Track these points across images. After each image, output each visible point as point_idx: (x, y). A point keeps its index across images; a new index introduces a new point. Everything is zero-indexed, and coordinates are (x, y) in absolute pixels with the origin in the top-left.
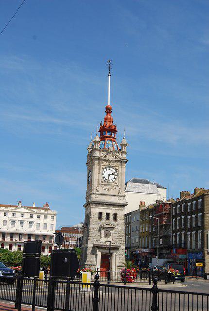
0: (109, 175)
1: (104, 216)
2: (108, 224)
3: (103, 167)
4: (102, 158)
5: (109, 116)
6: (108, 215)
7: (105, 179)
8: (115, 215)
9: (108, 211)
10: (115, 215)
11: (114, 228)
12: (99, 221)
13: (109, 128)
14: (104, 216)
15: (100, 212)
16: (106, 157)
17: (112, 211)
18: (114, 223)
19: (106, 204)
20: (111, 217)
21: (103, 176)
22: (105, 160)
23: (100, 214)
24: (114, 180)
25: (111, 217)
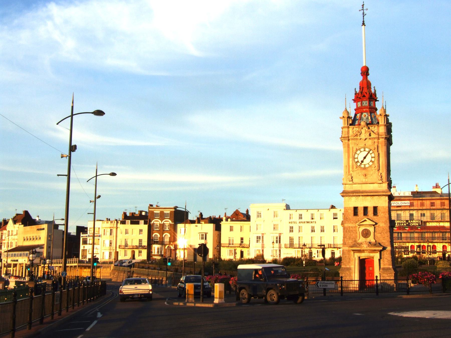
0: (365, 158)
1: (361, 212)
2: (365, 221)
8: (375, 209)
10: (375, 209)
12: (355, 217)
14: (361, 212)
15: (356, 206)
23: (356, 209)
24: (371, 163)
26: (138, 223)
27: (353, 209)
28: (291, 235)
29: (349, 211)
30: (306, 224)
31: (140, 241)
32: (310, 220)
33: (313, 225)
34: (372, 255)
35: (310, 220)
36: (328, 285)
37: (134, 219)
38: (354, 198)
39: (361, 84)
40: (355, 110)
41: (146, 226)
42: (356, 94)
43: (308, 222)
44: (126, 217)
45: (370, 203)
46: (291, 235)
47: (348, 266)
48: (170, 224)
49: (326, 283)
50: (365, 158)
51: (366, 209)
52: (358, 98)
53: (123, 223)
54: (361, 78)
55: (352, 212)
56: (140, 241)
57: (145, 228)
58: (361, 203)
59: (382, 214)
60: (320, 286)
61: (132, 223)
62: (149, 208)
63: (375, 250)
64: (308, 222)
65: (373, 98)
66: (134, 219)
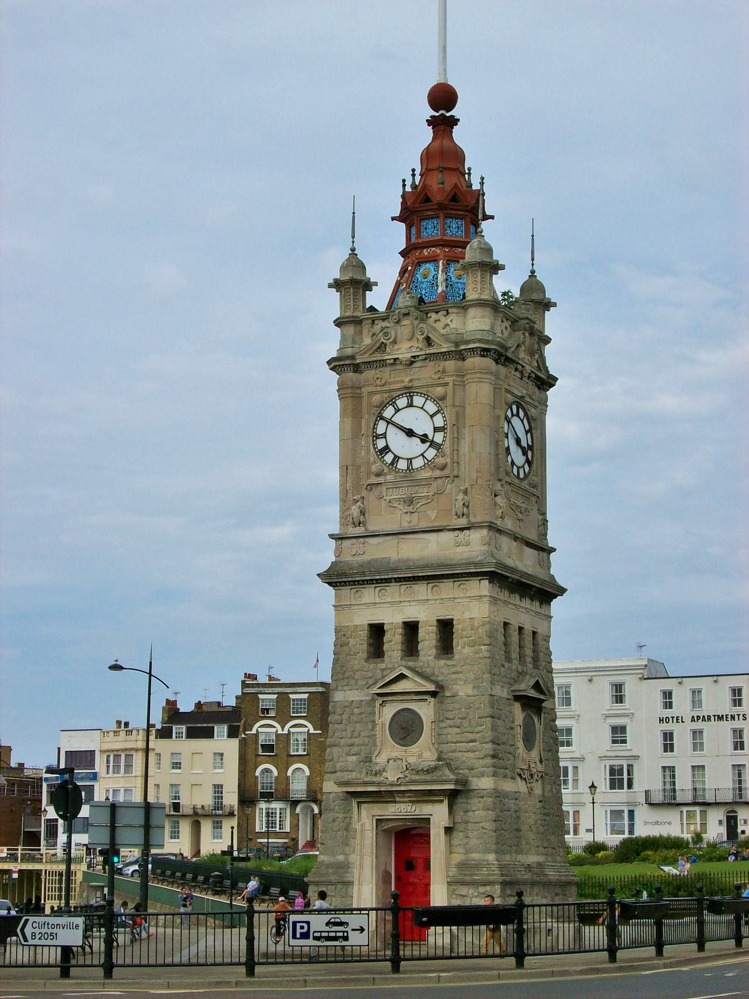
0: (410, 433)
1: (393, 642)
2: (402, 677)
3: (376, 399)
4: (366, 358)
5: (446, 143)
6: (411, 629)
7: (389, 458)
8: (446, 627)
9: (412, 613)
10: (446, 627)
11: (434, 694)
13: (454, 199)
14: (393, 642)
15: (376, 620)
16: (382, 347)
17: (422, 606)
18: (441, 667)
19: (398, 580)
20: (428, 638)
21: (381, 443)
22: (382, 363)
23: (377, 631)
25: (428, 638)
26: (208, 734)
27: (364, 634)
28: (669, 760)
29: (352, 641)
30: (713, 723)
31: (218, 789)
32: (726, 708)
33: (738, 724)
34: (425, 810)
35: (726, 708)
36: (60, 931)
37: (200, 722)
38: (369, 594)
39: (427, 156)
40: (403, 254)
41: (235, 743)
42: (404, 196)
43: (720, 718)
44: (173, 714)
45: (422, 606)
46: (669, 760)
47: (341, 858)
48: (309, 734)
49: (54, 926)
50: (410, 433)
51: (411, 629)
52: (414, 209)
53: (165, 733)
54: (427, 135)
55: (360, 643)
56: (218, 789)
57: (231, 747)
58: (392, 609)
59: (467, 650)
60: (33, 935)
61: (192, 734)
62: (244, 685)
63: (431, 792)
64: (720, 718)
65: (467, 207)
66: (200, 722)
